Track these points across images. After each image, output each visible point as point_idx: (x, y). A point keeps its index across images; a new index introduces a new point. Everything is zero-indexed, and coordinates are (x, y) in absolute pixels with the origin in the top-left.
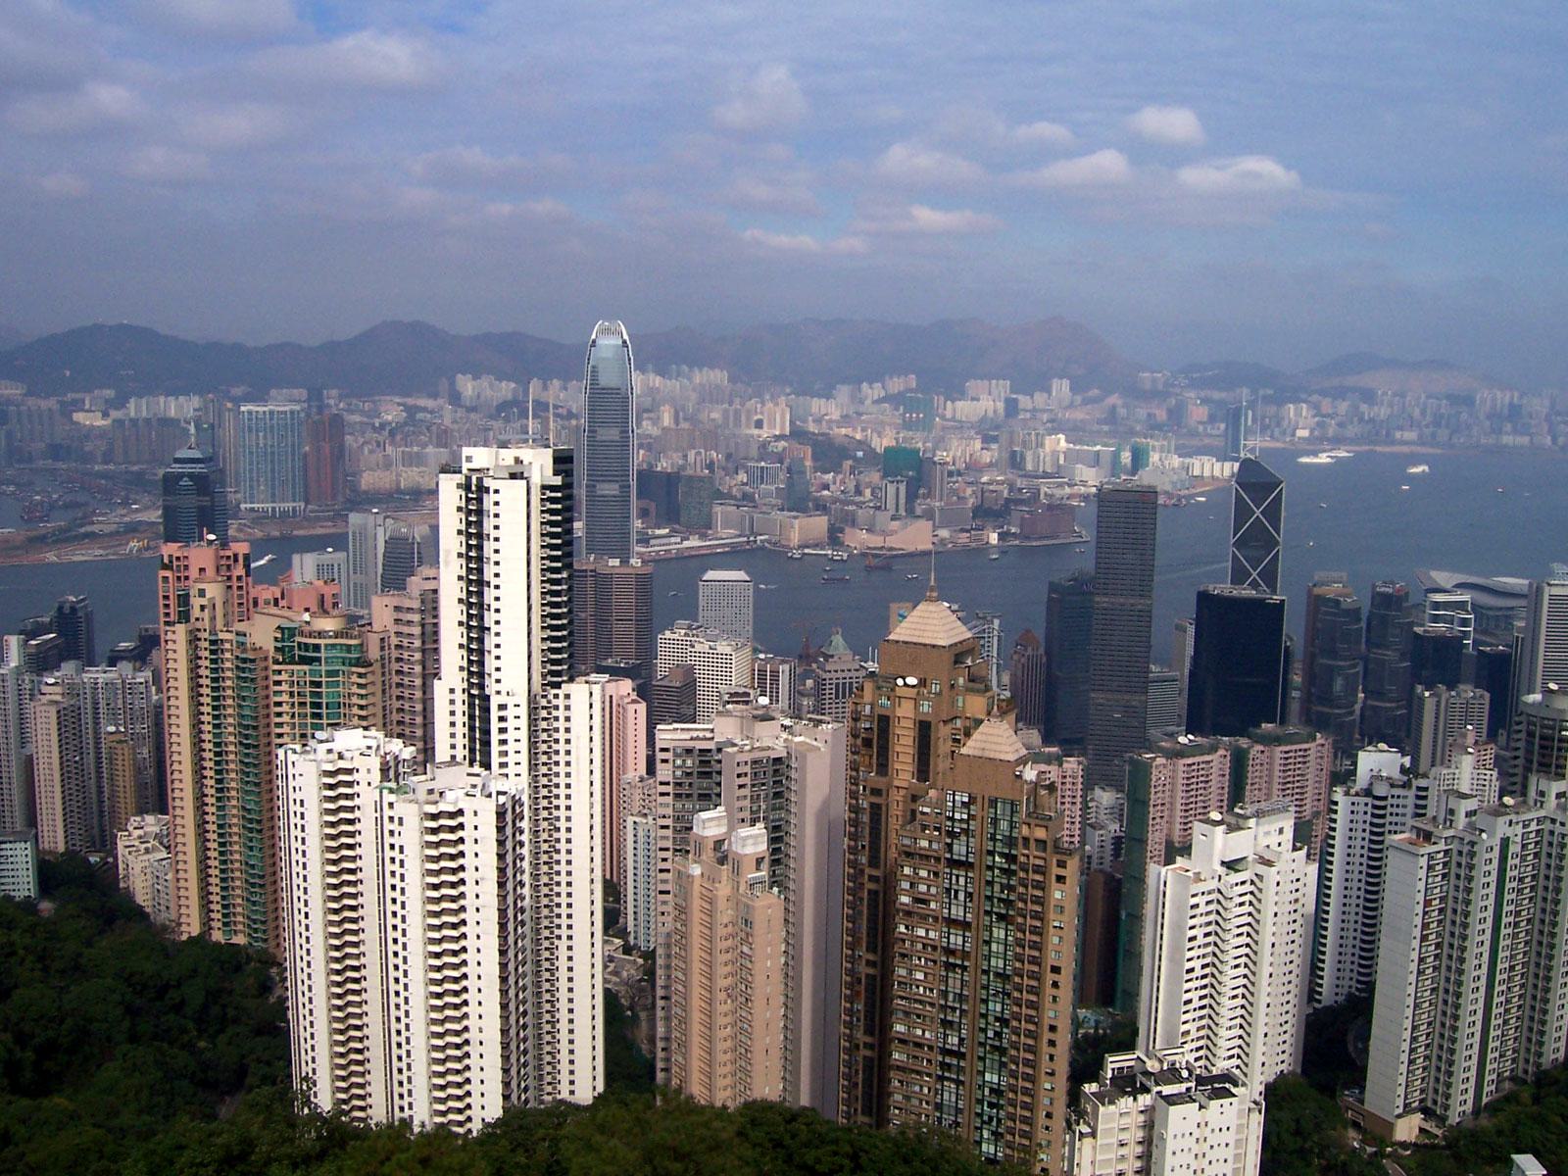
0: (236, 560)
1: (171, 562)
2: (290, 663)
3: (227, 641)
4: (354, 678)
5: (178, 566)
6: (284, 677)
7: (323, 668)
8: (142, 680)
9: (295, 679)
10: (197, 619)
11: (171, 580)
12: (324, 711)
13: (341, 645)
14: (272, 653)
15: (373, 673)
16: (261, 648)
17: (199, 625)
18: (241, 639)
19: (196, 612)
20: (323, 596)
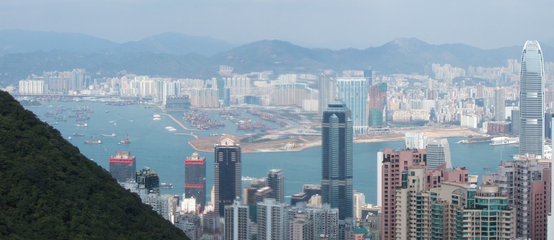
0: (420, 158)
1: (389, 158)
2: (471, 209)
3: (426, 197)
4: (504, 216)
5: (392, 160)
6: (469, 215)
7: (489, 211)
8: (335, 213)
9: (474, 216)
10: (411, 187)
11: (389, 167)
12: (488, 232)
13: (498, 200)
14: (450, 203)
15: (513, 213)
16: (445, 201)
17: (412, 189)
18: (434, 196)
19: (410, 183)
20: (460, 175)
